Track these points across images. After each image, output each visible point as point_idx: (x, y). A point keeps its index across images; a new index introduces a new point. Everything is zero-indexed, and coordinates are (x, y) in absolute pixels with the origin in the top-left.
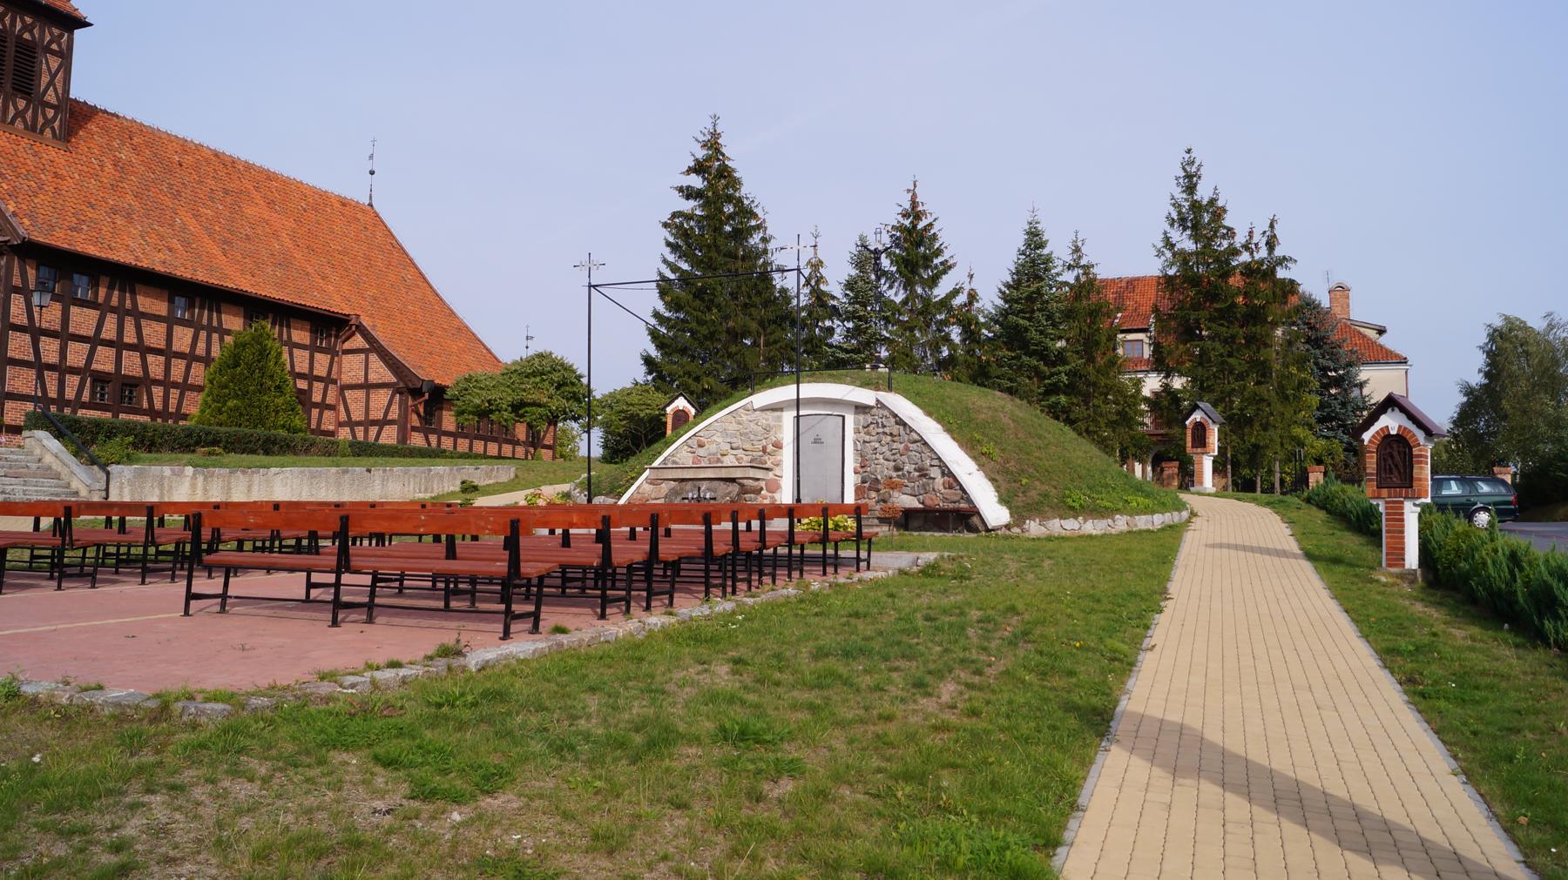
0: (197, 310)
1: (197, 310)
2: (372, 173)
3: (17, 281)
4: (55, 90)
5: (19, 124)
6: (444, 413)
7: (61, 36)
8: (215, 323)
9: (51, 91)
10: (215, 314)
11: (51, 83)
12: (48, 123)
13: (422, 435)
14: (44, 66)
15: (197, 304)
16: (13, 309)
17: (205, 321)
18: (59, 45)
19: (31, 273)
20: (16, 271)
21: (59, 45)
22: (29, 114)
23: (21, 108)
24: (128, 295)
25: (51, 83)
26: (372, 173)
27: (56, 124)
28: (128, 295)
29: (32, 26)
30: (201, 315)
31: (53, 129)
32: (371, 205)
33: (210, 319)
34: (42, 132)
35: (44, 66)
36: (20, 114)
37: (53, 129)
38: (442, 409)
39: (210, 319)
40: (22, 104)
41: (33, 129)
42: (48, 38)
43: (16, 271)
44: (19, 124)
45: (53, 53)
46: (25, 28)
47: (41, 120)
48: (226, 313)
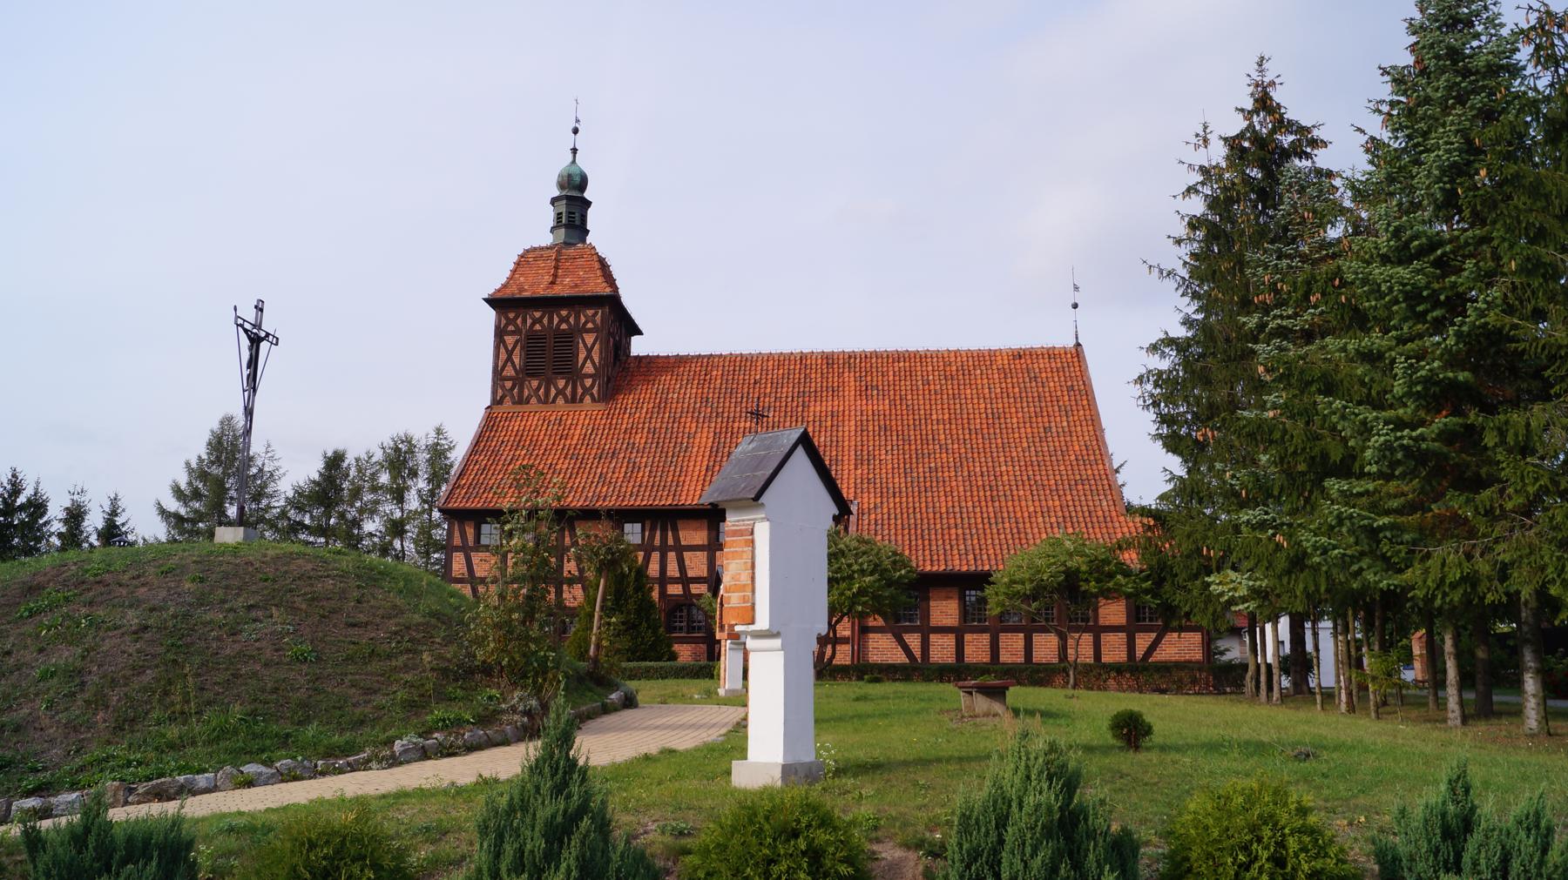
0: (647, 534)
1: (647, 534)
2: (1075, 306)
3: (457, 541)
4: (593, 363)
5: (560, 401)
6: (931, 603)
7: (595, 315)
8: (671, 542)
9: (589, 364)
10: (670, 534)
11: (589, 356)
12: (586, 391)
13: (889, 635)
14: (581, 345)
15: (648, 527)
16: (455, 566)
17: (657, 542)
18: (594, 322)
19: (470, 532)
20: (457, 534)
21: (594, 322)
22: (569, 388)
23: (561, 387)
24: (567, 533)
25: (589, 356)
26: (1075, 306)
27: (595, 391)
28: (567, 533)
29: (568, 317)
30: (652, 537)
31: (592, 395)
32: (1078, 345)
33: (664, 538)
34: (581, 400)
35: (581, 345)
36: (560, 392)
37: (592, 395)
38: (928, 599)
39: (664, 538)
40: (561, 383)
41: (573, 400)
42: (583, 320)
43: (457, 534)
44: (560, 401)
45: (589, 331)
46: (562, 320)
47: (580, 391)
48: (684, 529)
